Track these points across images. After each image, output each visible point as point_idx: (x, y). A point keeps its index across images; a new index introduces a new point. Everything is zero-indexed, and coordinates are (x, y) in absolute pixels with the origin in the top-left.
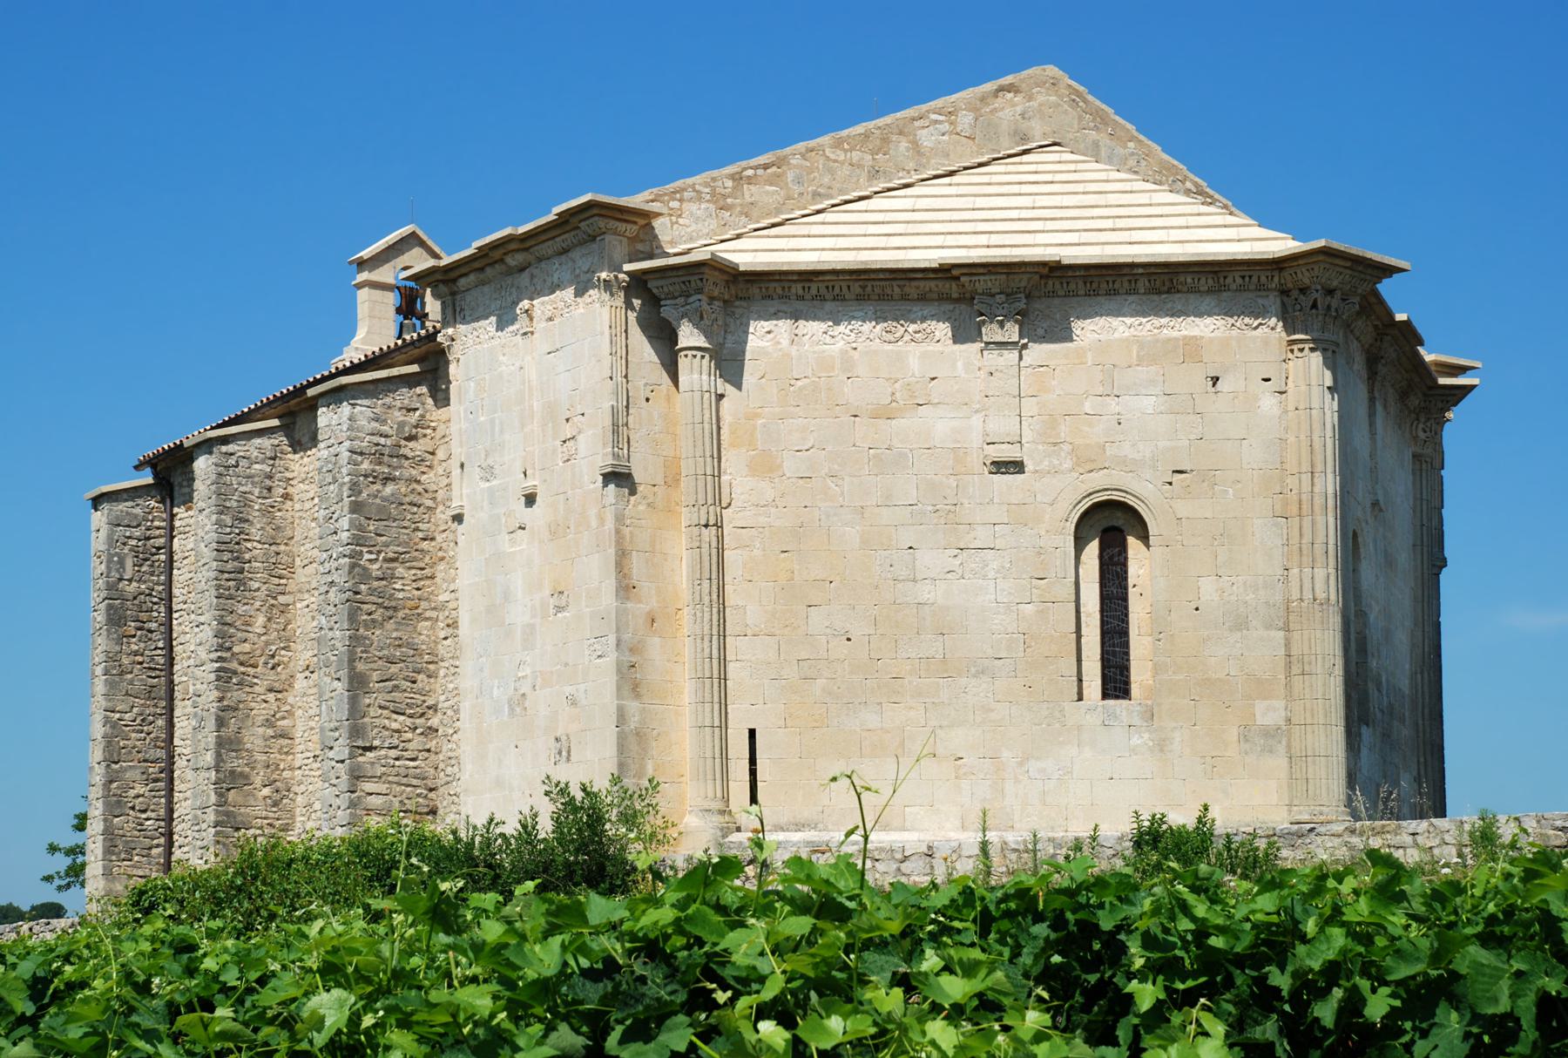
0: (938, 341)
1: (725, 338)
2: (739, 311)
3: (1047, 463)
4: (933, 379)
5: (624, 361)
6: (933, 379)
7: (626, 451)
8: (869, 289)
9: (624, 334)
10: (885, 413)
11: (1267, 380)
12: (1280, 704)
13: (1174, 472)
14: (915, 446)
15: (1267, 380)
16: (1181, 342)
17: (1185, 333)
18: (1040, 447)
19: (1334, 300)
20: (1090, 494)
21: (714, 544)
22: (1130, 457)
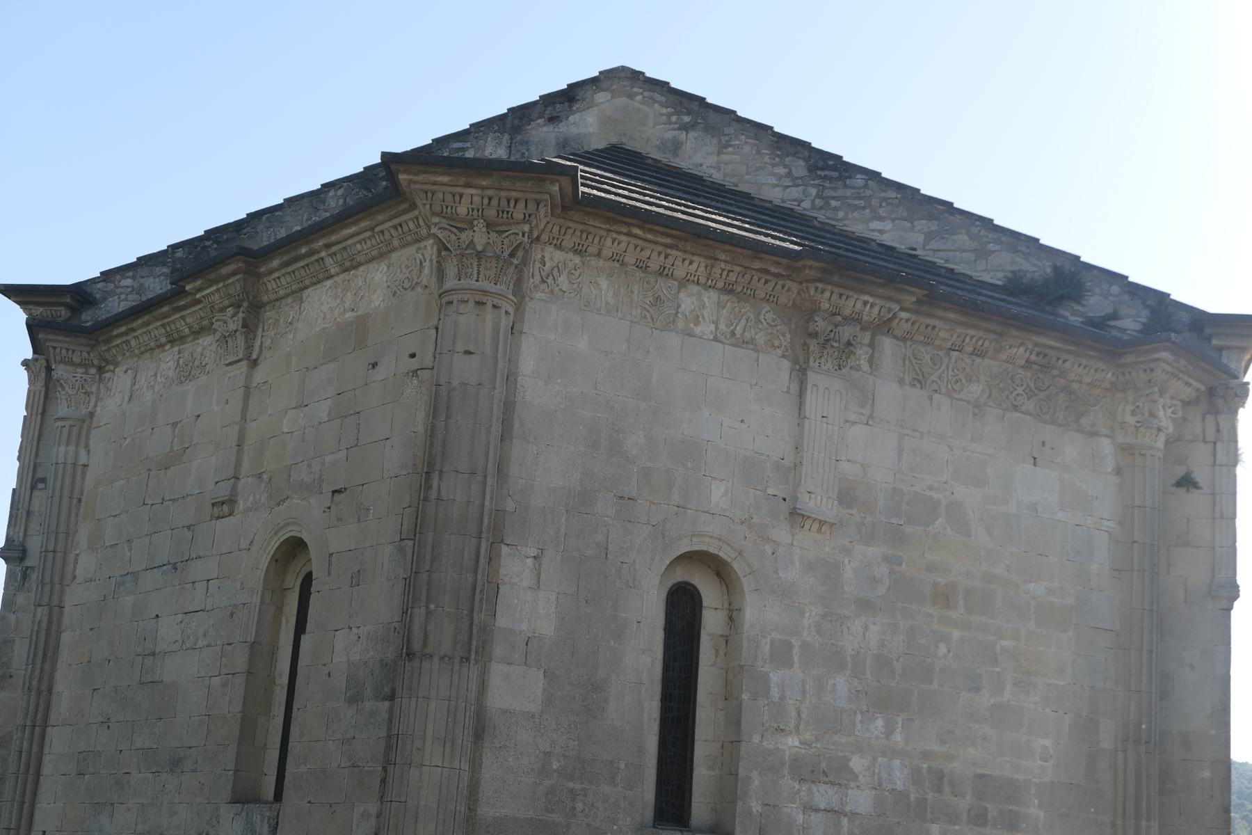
0: (208, 372)
1: (96, 406)
2: (107, 375)
3: (251, 498)
4: (199, 416)
5: (35, 443)
6: (199, 416)
7: (21, 534)
8: (168, 329)
9: (39, 417)
10: (168, 462)
11: (413, 356)
12: (373, 808)
13: (334, 492)
14: (176, 496)
15: (413, 356)
16: (355, 326)
17: (359, 313)
18: (250, 480)
19: (476, 235)
20: (276, 533)
21: (44, 625)
22: (305, 480)
